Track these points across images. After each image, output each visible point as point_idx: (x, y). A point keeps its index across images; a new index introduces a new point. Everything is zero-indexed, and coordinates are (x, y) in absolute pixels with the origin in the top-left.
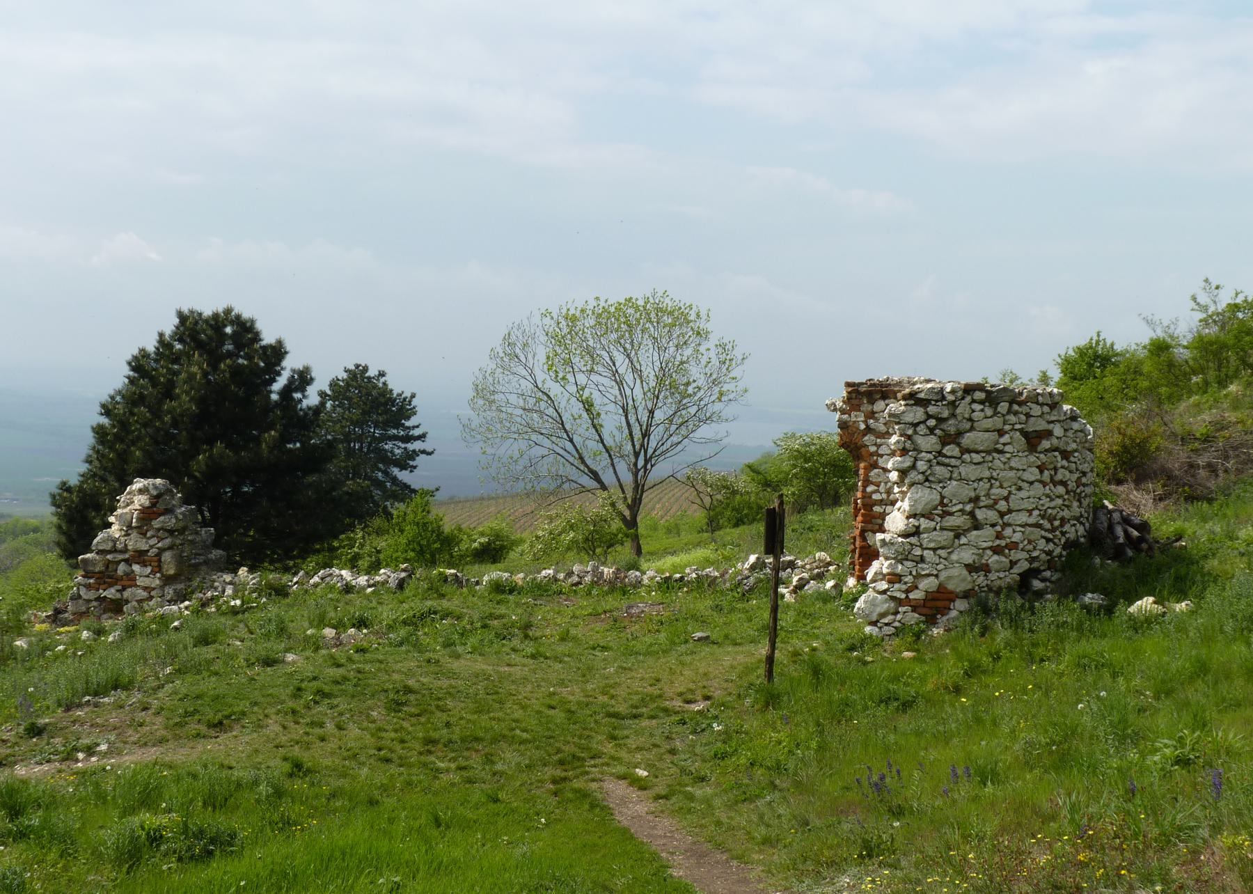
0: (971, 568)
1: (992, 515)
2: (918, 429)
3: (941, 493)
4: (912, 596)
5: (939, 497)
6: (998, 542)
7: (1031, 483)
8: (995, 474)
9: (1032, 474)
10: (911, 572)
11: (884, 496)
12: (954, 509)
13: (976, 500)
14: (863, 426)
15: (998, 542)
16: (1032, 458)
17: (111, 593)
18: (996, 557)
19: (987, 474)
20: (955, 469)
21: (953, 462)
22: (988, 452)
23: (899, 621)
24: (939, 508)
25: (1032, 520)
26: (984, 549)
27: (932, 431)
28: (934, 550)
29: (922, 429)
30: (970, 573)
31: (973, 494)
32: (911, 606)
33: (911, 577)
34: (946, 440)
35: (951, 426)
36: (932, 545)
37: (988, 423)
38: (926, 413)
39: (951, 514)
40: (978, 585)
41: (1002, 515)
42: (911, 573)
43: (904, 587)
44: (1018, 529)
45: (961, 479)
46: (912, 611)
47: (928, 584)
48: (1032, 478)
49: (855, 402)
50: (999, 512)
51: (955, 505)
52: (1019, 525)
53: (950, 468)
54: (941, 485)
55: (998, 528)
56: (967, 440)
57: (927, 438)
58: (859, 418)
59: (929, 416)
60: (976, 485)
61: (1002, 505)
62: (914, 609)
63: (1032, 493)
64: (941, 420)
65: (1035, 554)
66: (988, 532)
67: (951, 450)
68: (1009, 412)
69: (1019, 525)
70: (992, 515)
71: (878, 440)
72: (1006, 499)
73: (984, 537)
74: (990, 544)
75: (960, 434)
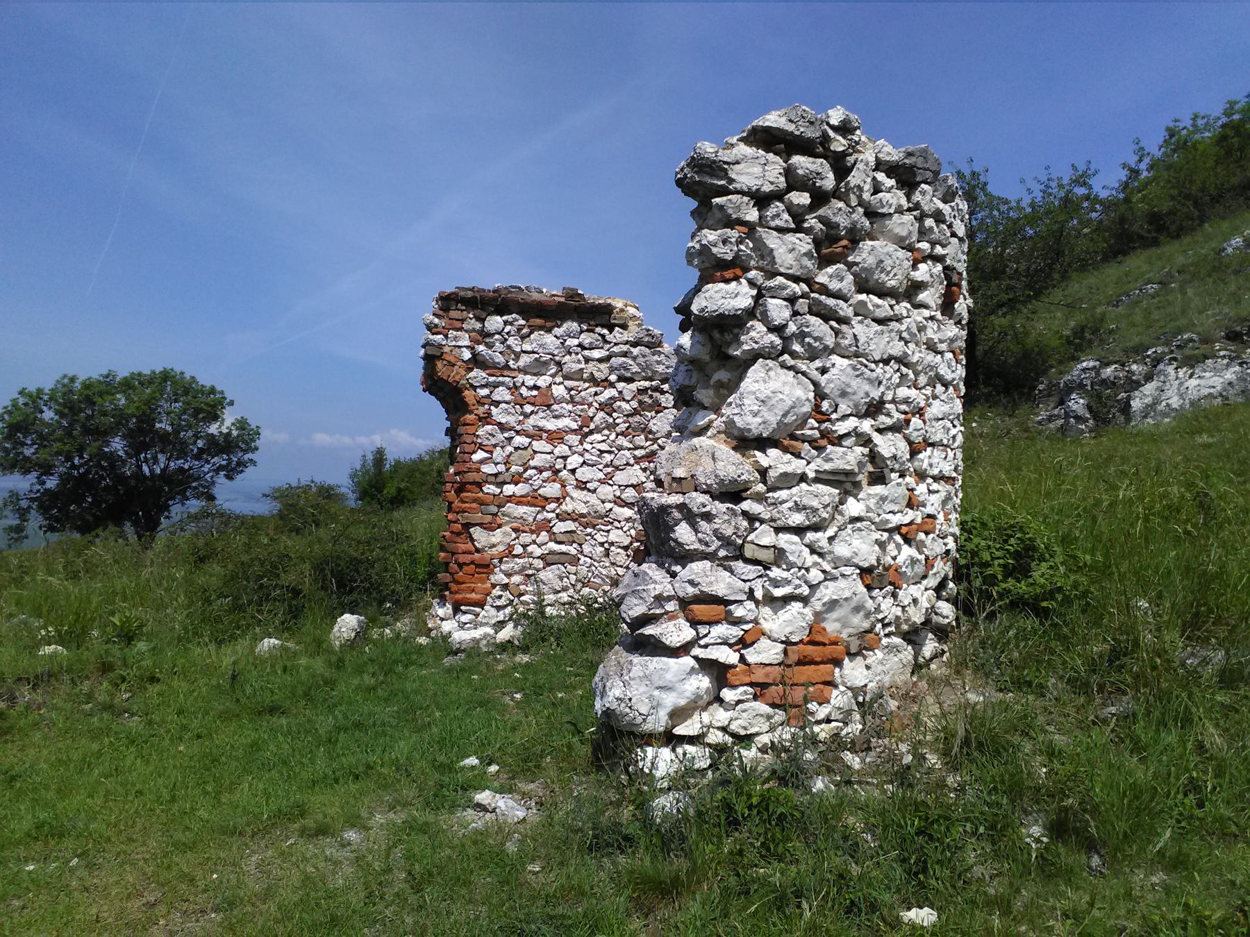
2: (770, 212)
3: (816, 384)
4: (752, 656)
5: (812, 395)
6: (910, 515)
10: (751, 591)
11: (501, 468)
12: (842, 428)
14: (467, 355)
20: (844, 328)
23: (724, 729)
24: (812, 422)
26: (890, 531)
27: (798, 215)
28: (799, 531)
29: (778, 213)
30: (869, 588)
32: (751, 684)
33: (750, 605)
35: (837, 211)
36: (797, 519)
38: (789, 172)
39: (838, 440)
40: (882, 620)
41: (914, 453)
42: (751, 595)
43: (735, 632)
45: (857, 355)
46: (755, 697)
49: (453, 314)
50: (910, 443)
51: (845, 417)
53: (833, 323)
54: (818, 363)
57: (791, 238)
58: (461, 344)
59: (794, 181)
60: (879, 370)
62: (760, 690)
64: (820, 198)
66: (895, 487)
71: (492, 379)
75: (855, 237)
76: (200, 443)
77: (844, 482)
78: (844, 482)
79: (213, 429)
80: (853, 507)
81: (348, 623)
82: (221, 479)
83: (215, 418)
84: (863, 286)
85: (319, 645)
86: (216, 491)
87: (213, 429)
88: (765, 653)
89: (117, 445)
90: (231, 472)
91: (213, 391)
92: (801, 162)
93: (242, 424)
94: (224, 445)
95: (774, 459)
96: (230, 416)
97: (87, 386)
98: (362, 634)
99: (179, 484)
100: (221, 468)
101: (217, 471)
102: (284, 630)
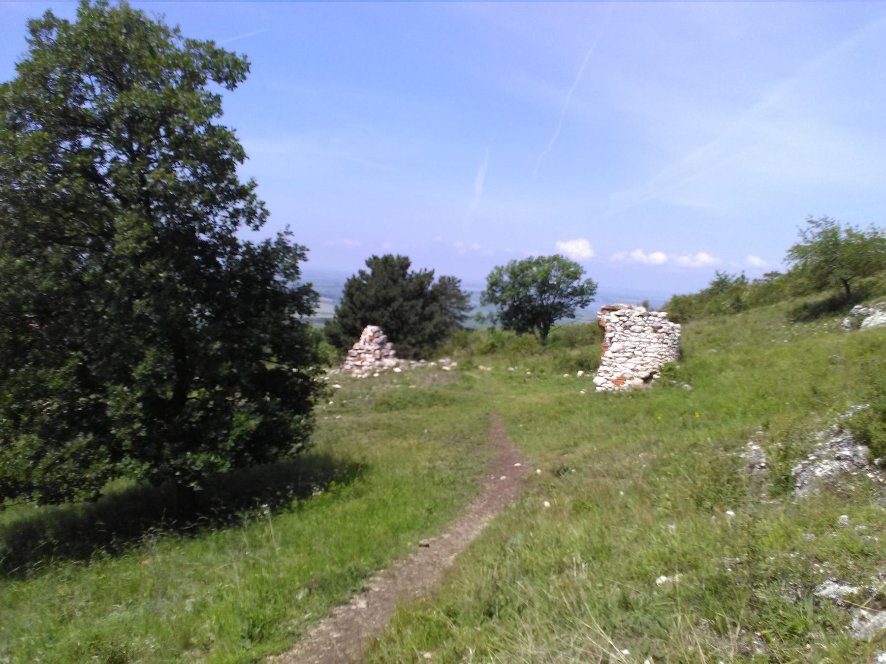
0: (633, 370)
1: (640, 353)
9: (655, 340)
17: (358, 363)
34: (626, 328)
35: (628, 323)
47: (618, 375)
56: (632, 328)
61: (644, 350)
66: (638, 358)
67: (627, 331)
70: (640, 353)
73: (637, 360)
75: (630, 326)
76: (569, 290)
77: (629, 358)
78: (629, 358)
79: (575, 284)
80: (630, 360)
81: (580, 373)
82: (578, 308)
83: (576, 278)
84: (633, 332)
85: (575, 376)
86: (576, 313)
87: (575, 284)
88: (614, 378)
89: (533, 291)
90: (584, 304)
91: (576, 265)
92: (621, 318)
93: (589, 282)
94: (581, 292)
95: (617, 355)
96: (583, 278)
97: (521, 264)
98: (583, 375)
99: (559, 310)
100: (579, 302)
101: (576, 304)
102: (570, 373)
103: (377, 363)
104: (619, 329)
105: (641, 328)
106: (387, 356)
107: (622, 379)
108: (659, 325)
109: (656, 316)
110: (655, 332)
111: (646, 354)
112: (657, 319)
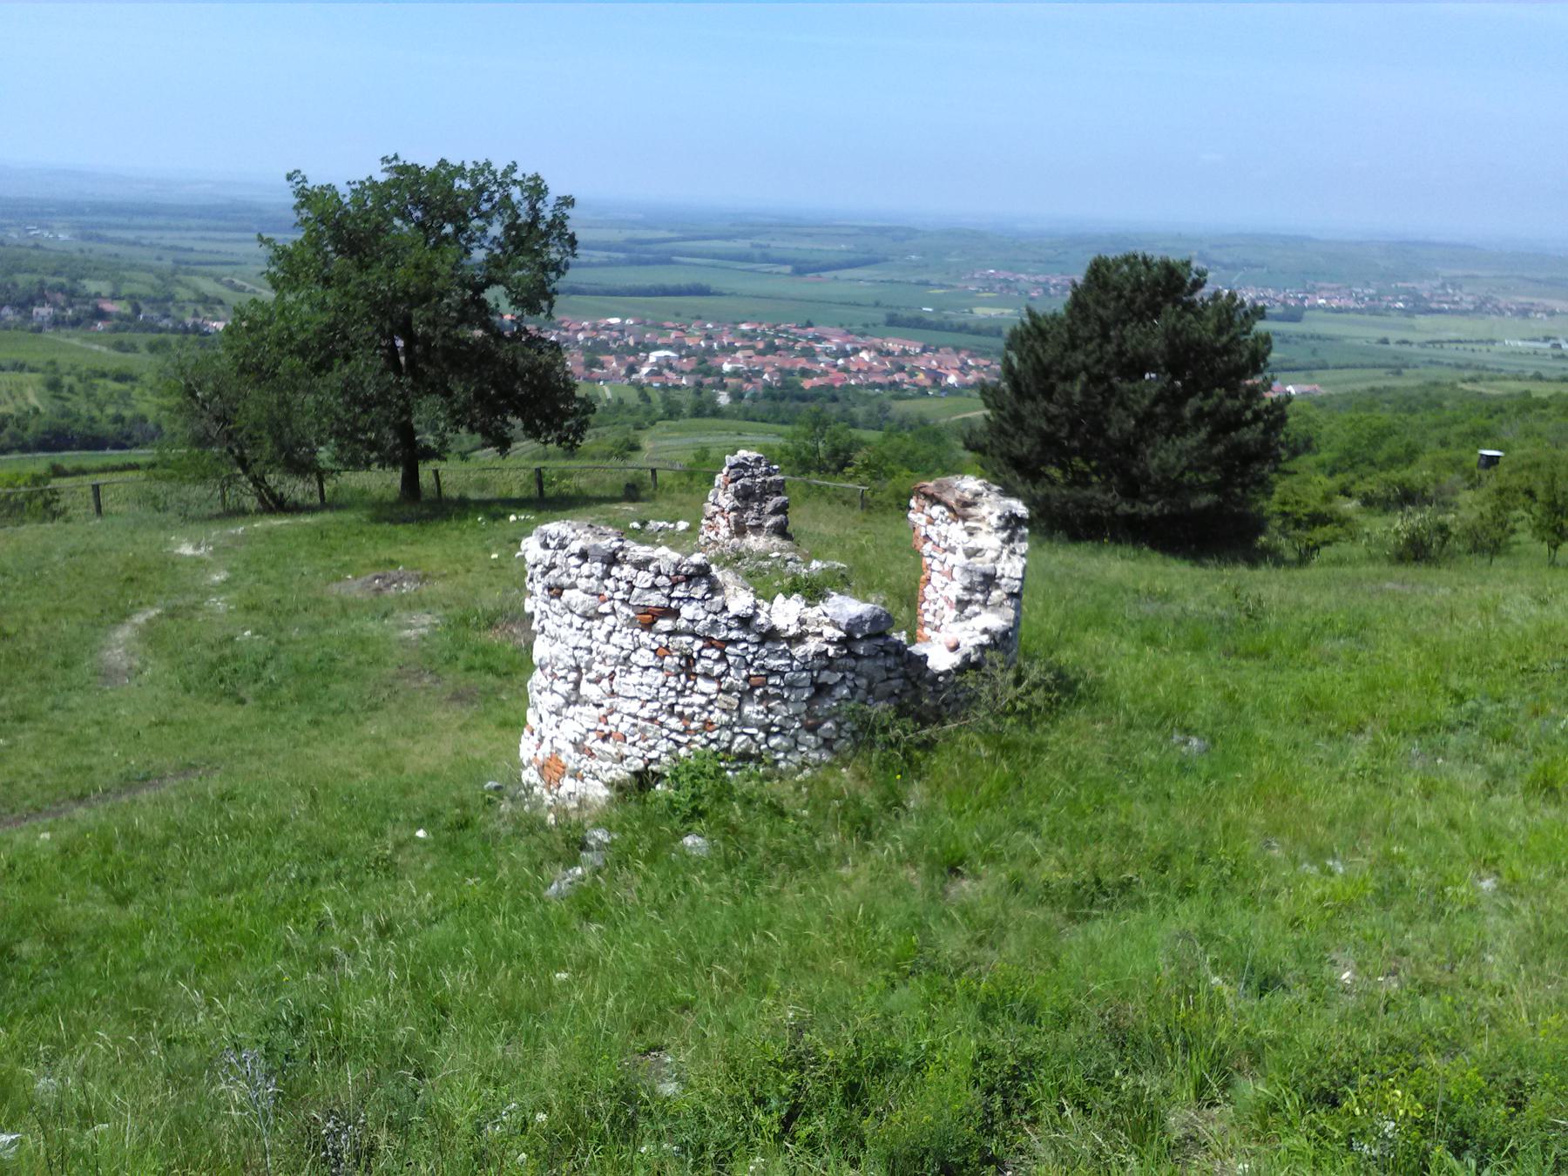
6: (601, 726)
7: (647, 668)
8: (594, 647)
9: (644, 657)
12: (560, 674)
13: (578, 669)
15: (601, 726)
16: (645, 637)
17: (712, 535)
18: (599, 744)
19: (585, 643)
21: (556, 618)
22: (590, 619)
25: (645, 713)
26: (589, 730)
31: (573, 663)
37: (582, 583)
44: (626, 718)
48: (644, 663)
52: (629, 714)
55: (603, 711)
63: (645, 680)
65: (654, 754)
68: (607, 575)
69: (629, 714)
72: (612, 676)
74: (592, 726)
103: (736, 540)
104: (538, 588)
105: (591, 601)
106: (757, 529)
107: (552, 770)
108: (655, 599)
109: (642, 565)
110: (648, 627)
111: (619, 703)
112: (644, 579)
